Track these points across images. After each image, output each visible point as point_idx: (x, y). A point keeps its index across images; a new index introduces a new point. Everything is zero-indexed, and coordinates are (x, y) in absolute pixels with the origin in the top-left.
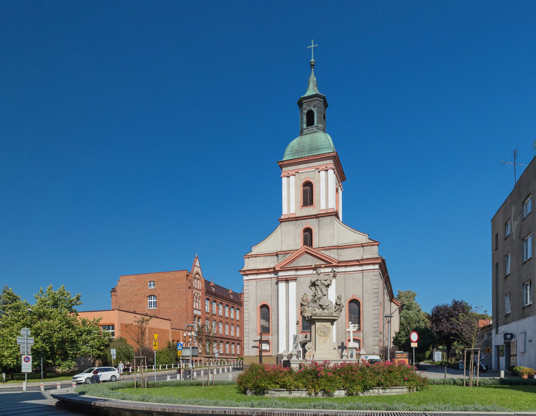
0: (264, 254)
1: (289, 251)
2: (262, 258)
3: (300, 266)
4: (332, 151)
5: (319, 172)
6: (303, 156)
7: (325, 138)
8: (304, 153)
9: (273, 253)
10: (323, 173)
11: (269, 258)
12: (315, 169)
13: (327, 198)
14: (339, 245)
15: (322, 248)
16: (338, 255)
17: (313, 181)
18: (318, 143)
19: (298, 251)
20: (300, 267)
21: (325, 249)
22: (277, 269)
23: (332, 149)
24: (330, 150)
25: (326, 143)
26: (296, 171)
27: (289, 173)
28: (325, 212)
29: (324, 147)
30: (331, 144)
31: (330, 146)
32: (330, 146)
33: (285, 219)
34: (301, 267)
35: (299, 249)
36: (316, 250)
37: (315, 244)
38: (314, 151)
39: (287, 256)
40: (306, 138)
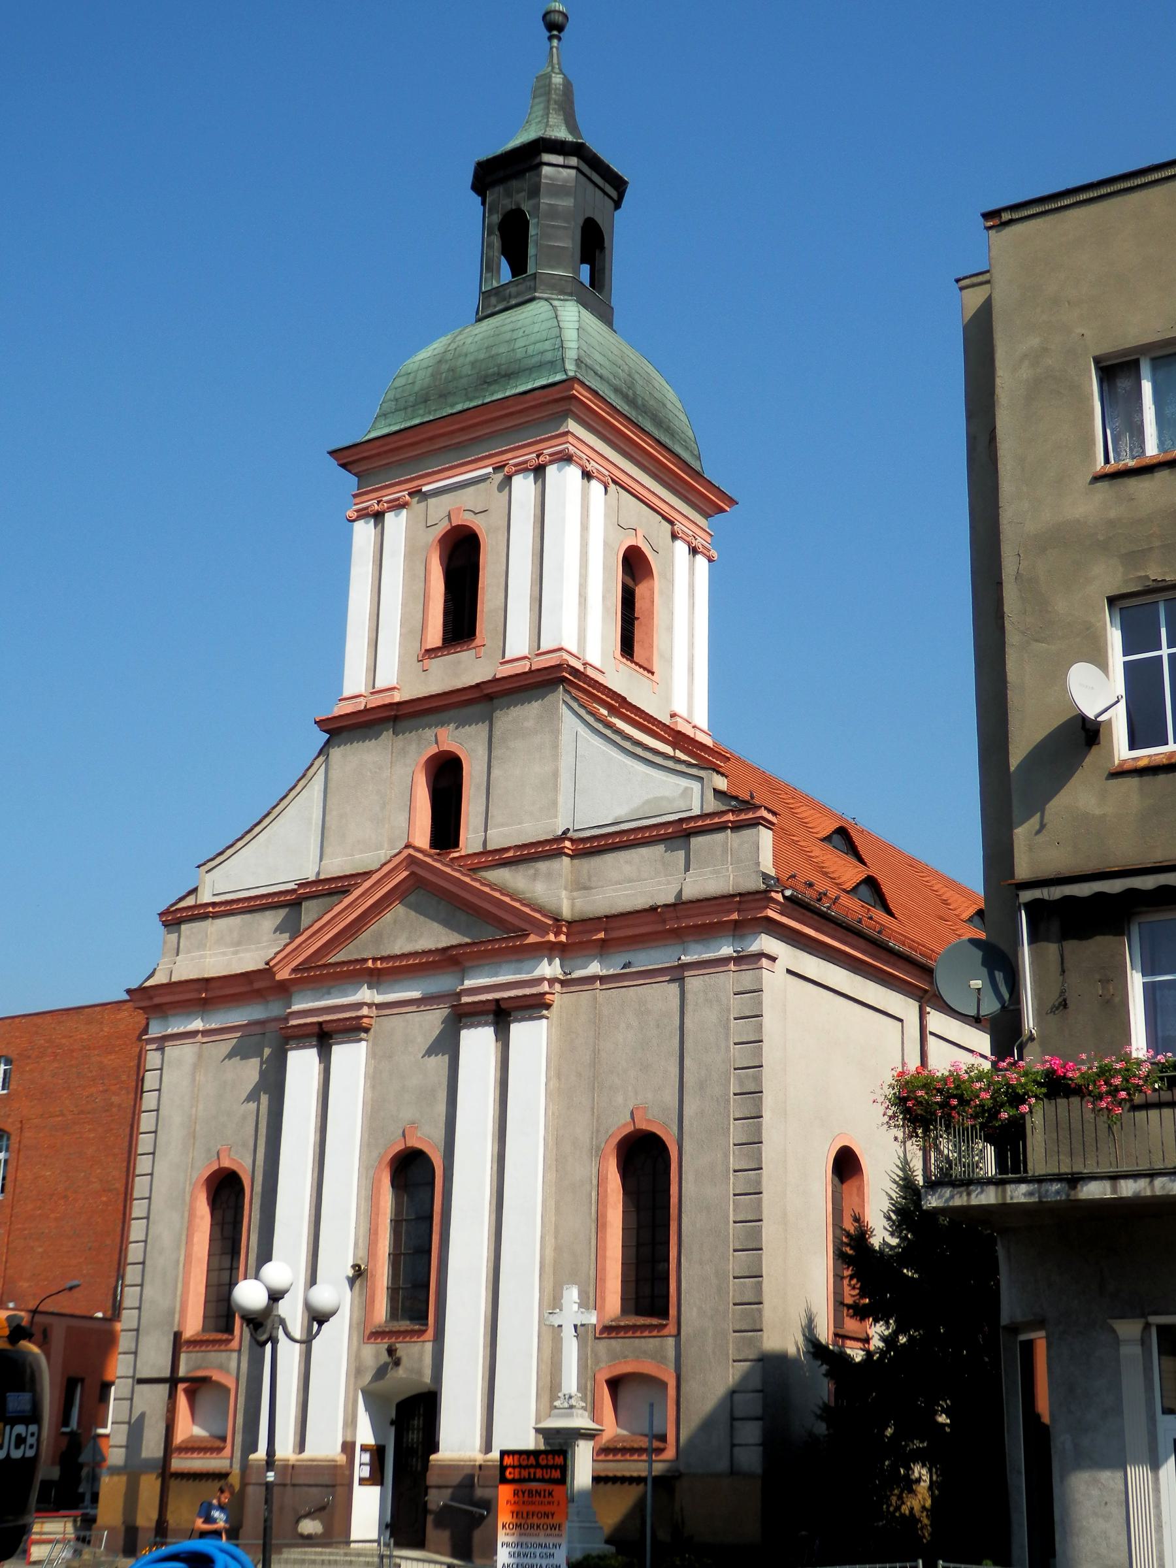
8: (450, 400)
16: (580, 886)
17: (479, 524)
19: (376, 877)
22: (283, 974)
35: (380, 869)
37: (470, 839)
38: (492, 388)
40: (476, 332)
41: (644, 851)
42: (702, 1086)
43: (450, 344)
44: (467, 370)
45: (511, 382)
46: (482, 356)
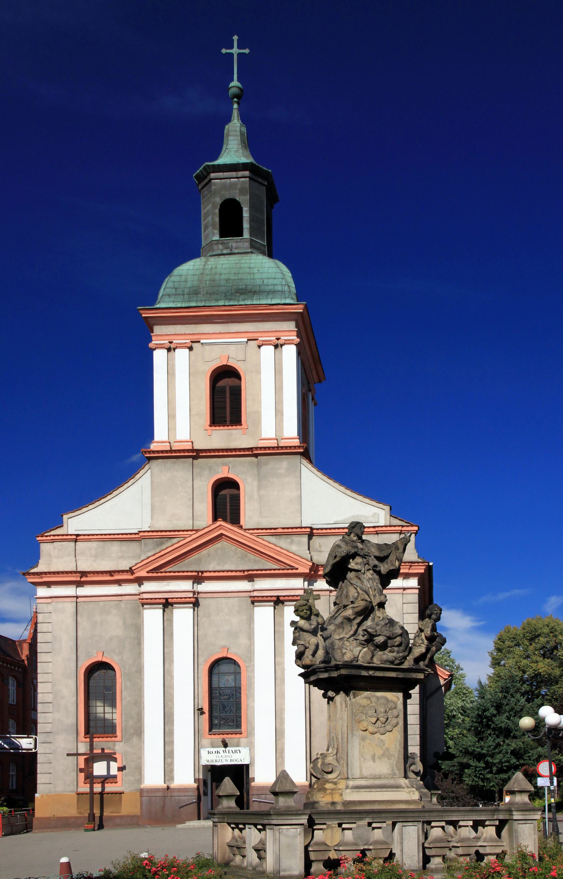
0: (101, 535)
1: (174, 531)
2: (94, 544)
3: (205, 569)
4: (292, 302)
5: (259, 347)
6: (212, 304)
7: (275, 270)
9: (127, 534)
10: (268, 351)
11: (115, 547)
13: (279, 412)
15: (269, 531)
18: (255, 277)
21: (275, 532)
22: (143, 573)
23: (294, 297)
24: (288, 297)
25: (276, 282)
27: (174, 341)
28: (273, 443)
29: (271, 288)
30: (290, 284)
31: (286, 288)
32: (286, 288)
33: (162, 452)
34: (210, 572)
38: (242, 297)
39: (169, 544)
40: (221, 262)
43: (205, 265)
44: (222, 283)
45: (255, 296)
46: (232, 277)
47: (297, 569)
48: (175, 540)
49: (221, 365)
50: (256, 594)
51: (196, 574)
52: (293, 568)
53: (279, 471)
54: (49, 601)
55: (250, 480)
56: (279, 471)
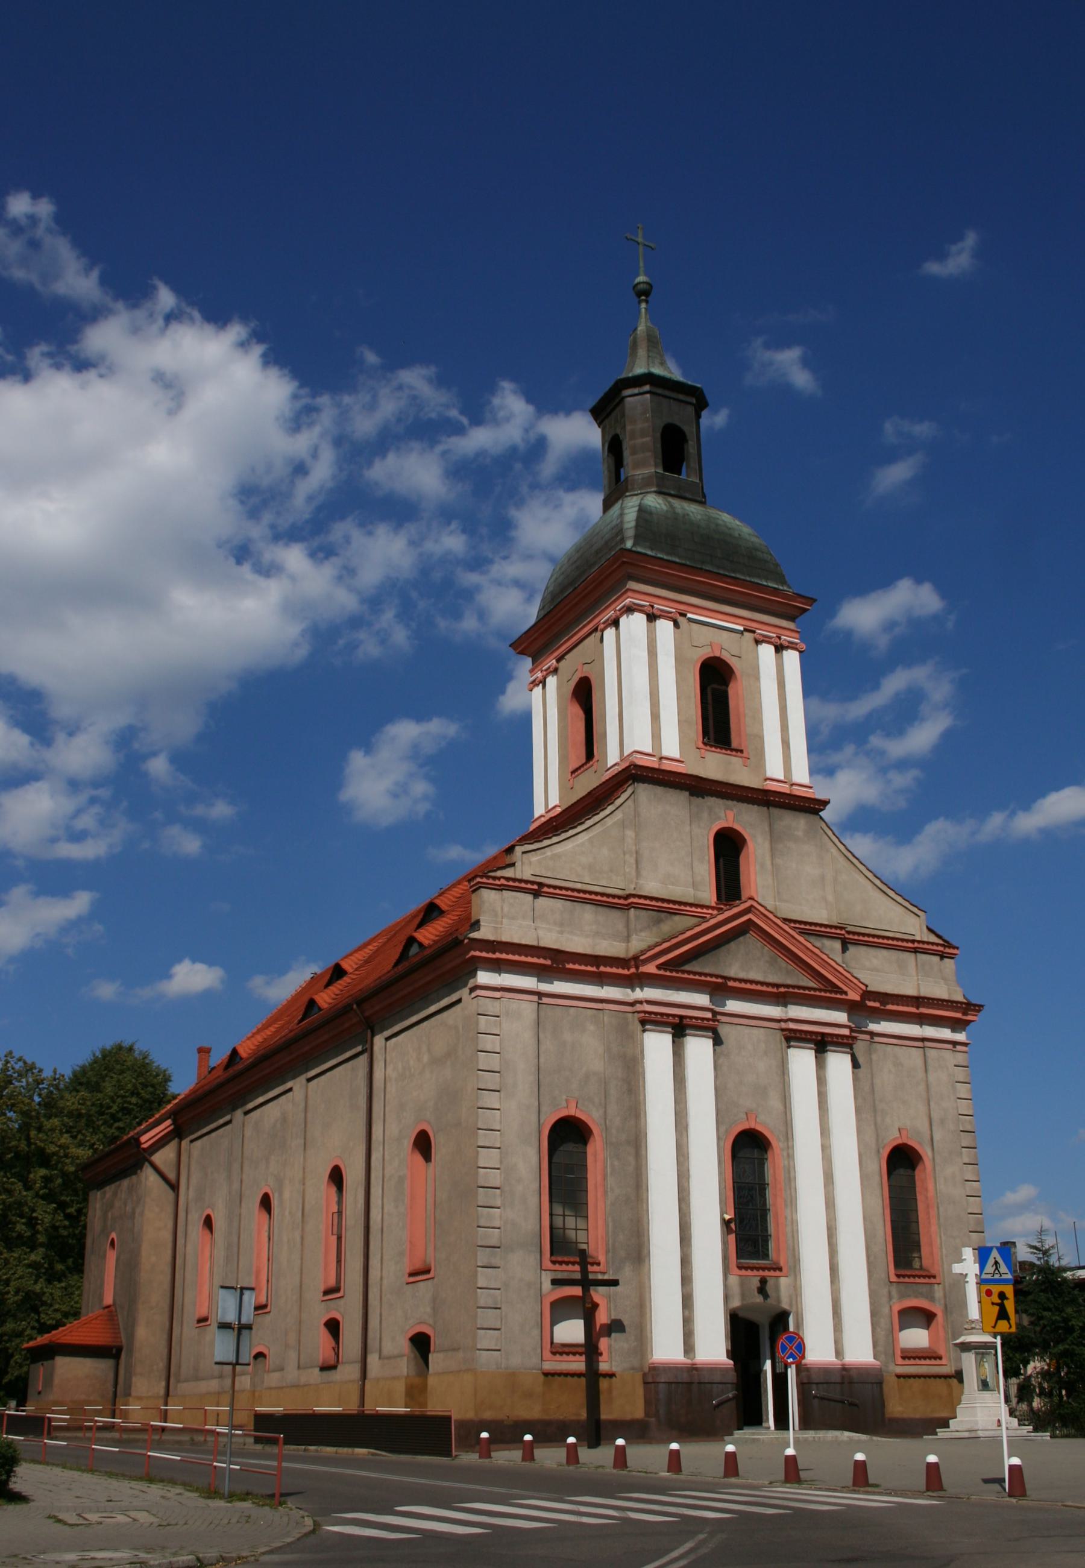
2: (558, 904)
5: (757, 642)
10: (766, 652)
11: (588, 914)
12: (742, 628)
14: (850, 929)
20: (730, 979)
26: (682, 607)
36: (794, 928)
41: (885, 952)
42: (942, 1121)
47: (846, 993)
48: (677, 918)
49: (712, 655)
50: (792, 1026)
51: (720, 980)
52: (836, 989)
53: (796, 833)
54: (498, 994)
55: (760, 840)
56: (796, 833)
